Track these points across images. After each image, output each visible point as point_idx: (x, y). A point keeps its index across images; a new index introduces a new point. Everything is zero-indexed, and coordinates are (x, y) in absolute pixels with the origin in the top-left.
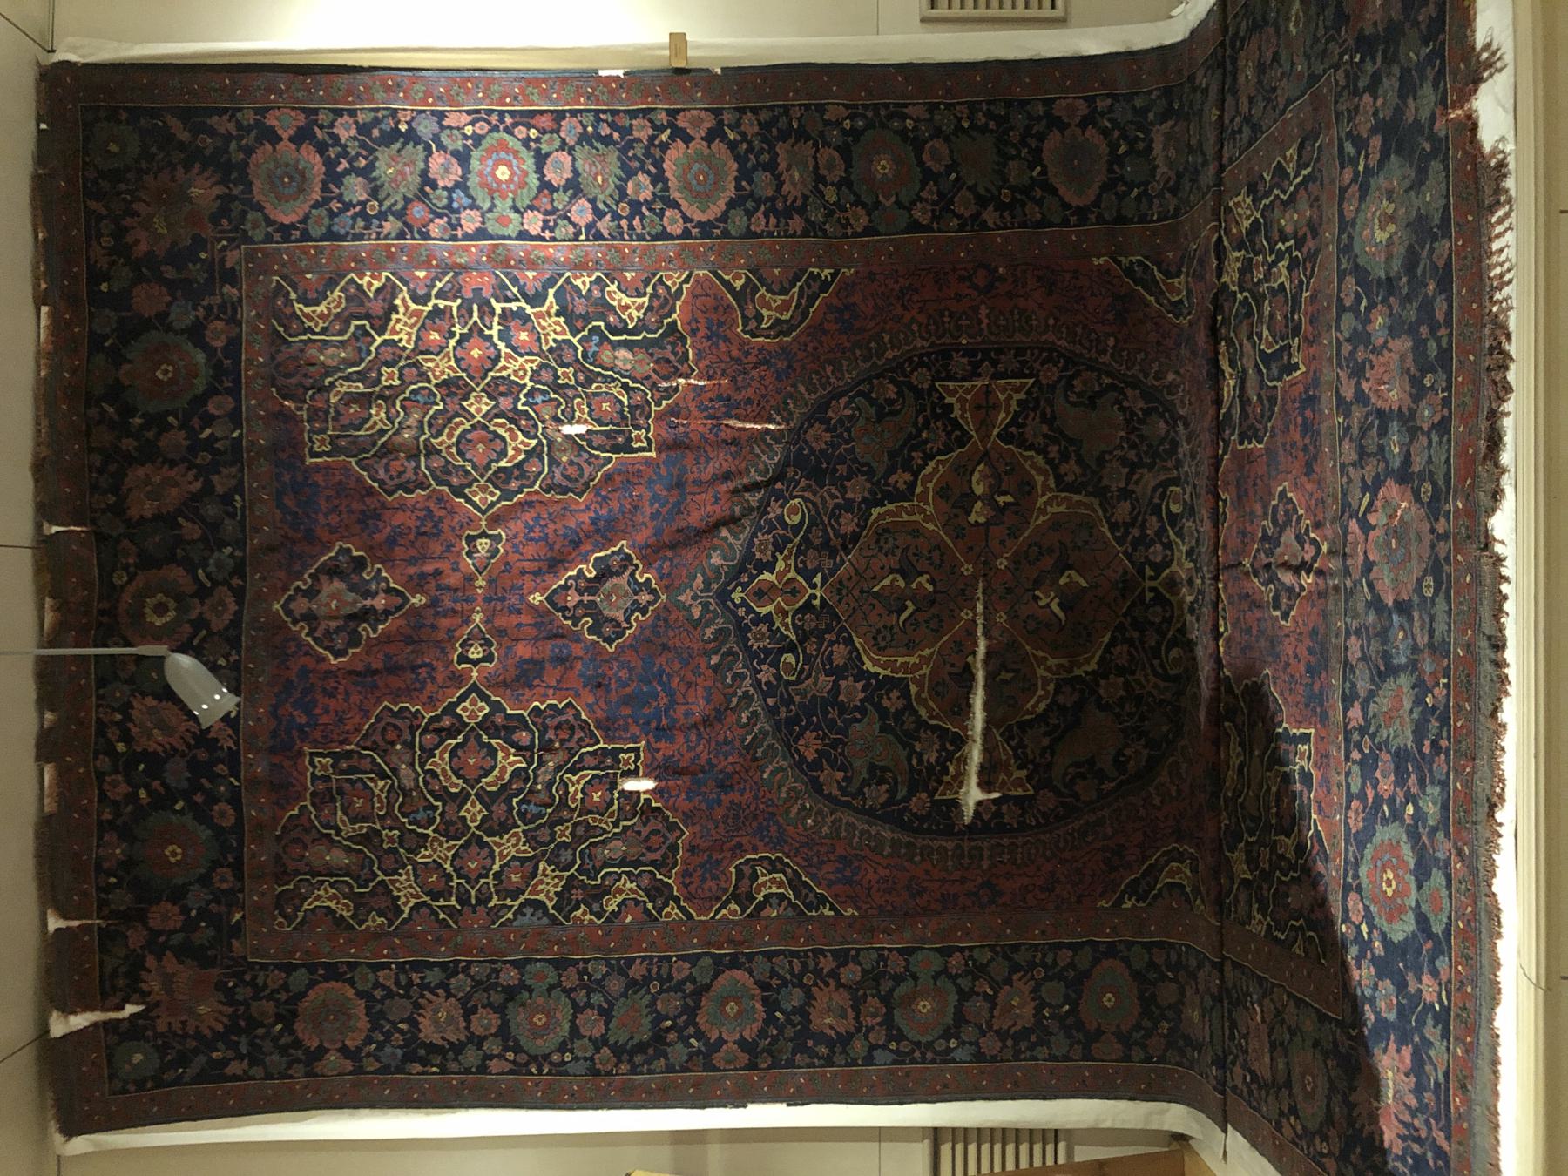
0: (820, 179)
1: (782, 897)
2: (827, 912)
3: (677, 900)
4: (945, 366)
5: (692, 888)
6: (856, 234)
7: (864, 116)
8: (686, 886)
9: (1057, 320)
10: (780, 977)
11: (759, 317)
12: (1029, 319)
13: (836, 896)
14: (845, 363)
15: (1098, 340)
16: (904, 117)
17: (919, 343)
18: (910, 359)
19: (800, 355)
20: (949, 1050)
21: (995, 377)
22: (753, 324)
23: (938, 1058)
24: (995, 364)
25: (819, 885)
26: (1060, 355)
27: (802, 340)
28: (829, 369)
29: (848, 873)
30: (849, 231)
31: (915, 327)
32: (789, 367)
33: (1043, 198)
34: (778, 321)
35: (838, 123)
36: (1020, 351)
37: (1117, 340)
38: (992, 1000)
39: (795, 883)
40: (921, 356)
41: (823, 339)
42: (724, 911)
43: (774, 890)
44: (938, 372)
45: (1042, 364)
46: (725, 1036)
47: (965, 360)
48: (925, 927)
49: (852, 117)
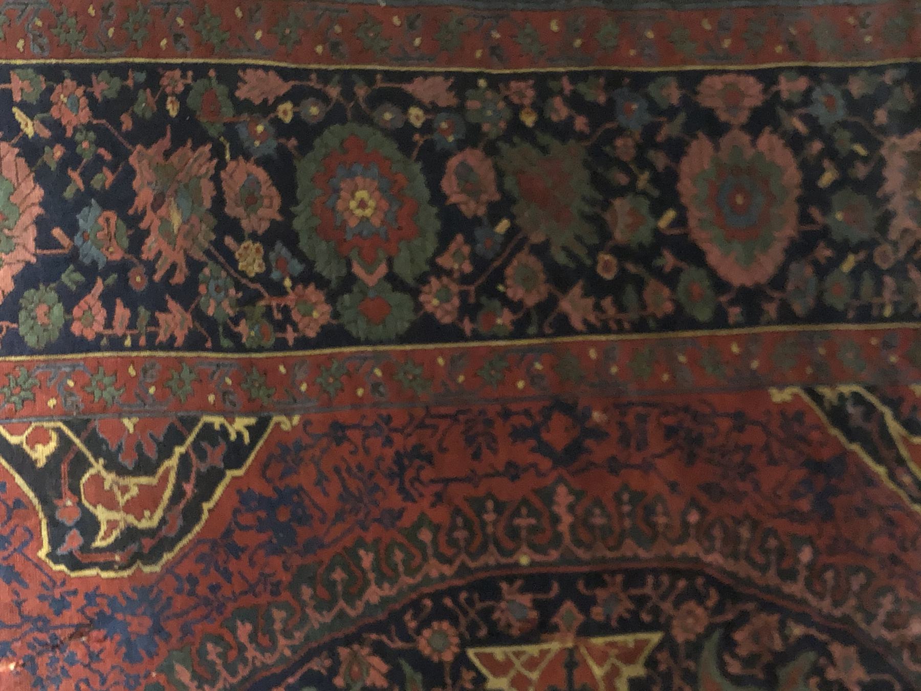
0: (227, 226)
4: (486, 614)
6: (303, 343)
7: (323, 98)
9: (703, 511)
11: (89, 526)
12: (649, 511)
14: (279, 615)
15: (782, 553)
16: (405, 101)
17: (434, 569)
18: (416, 605)
19: (180, 602)
21: (587, 630)
22: (73, 542)
24: (585, 605)
26: (711, 581)
27: (183, 570)
28: (244, 630)
30: (290, 336)
31: (426, 536)
32: (157, 629)
33: (677, 271)
34: (131, 534)
35: (266, 109)
36: (634, 577)
37: (816, 552)
40: (436, 597)
41: (233, 565)
44: (473, 627)
45: (677, 605)
47: (526, 600)
49: (295, 96)
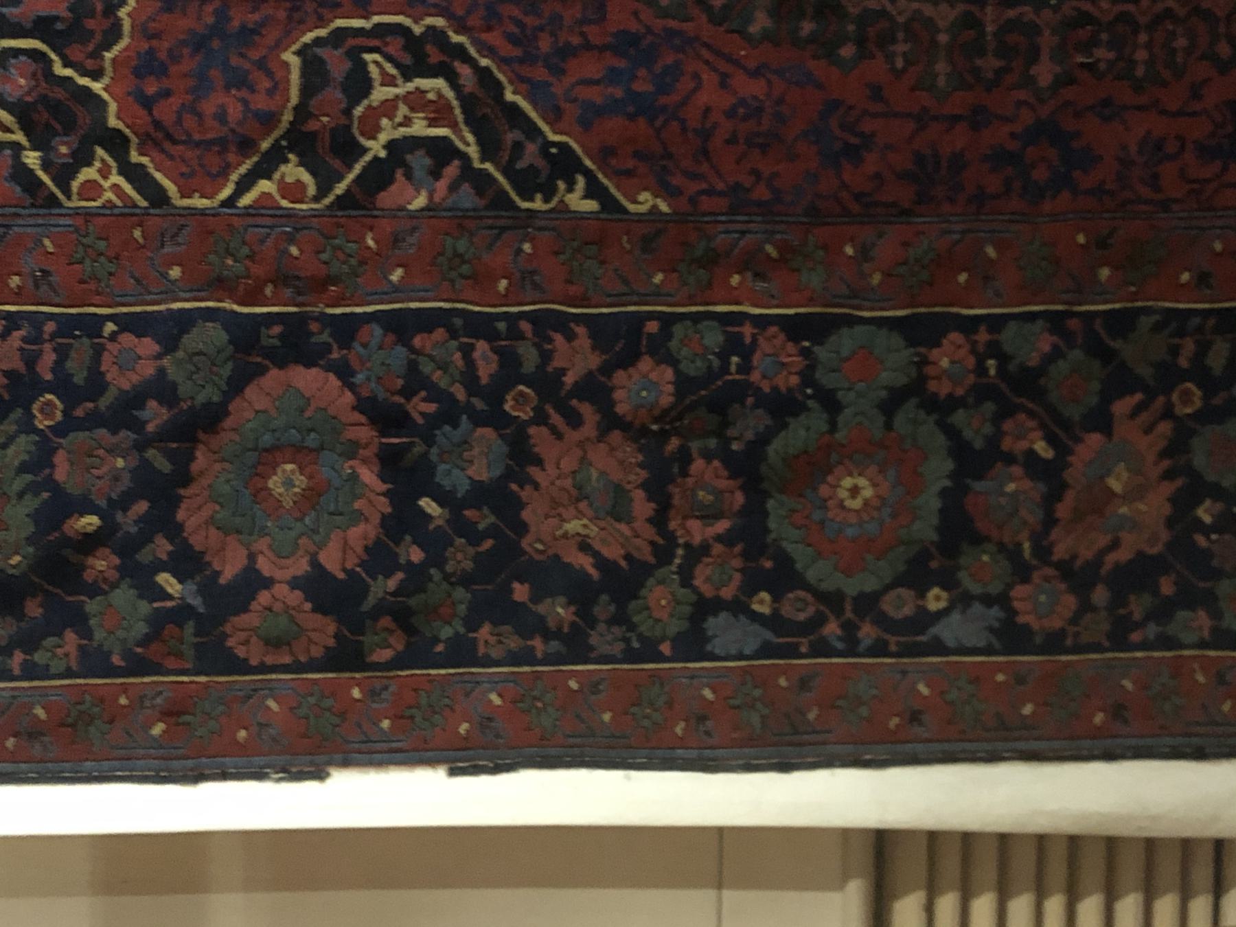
1: (441, 152)
2: (579, 202)
3: (116, 143)
5: (166, 111)
8: (147, 103)
10: (436, 394)
13: (604, 154)
20: (924, 619)
23: (893, 641)
25: (555, 116)
29: (643, 86)
38: (1050, 475)
39: (485, 111)
42: (265, 186)
43: (420, 128)
46: (264, 566)
48: (864, 253)
